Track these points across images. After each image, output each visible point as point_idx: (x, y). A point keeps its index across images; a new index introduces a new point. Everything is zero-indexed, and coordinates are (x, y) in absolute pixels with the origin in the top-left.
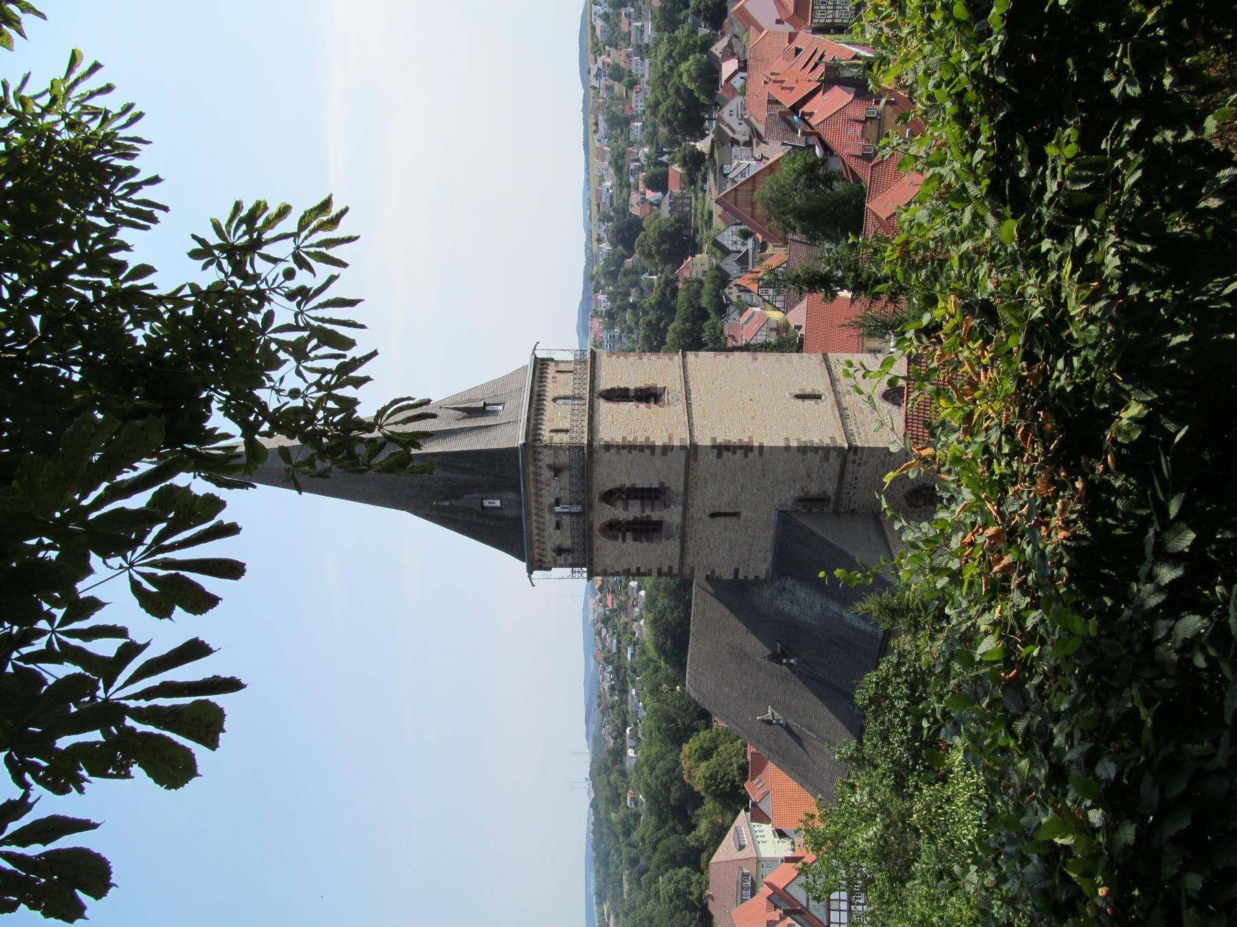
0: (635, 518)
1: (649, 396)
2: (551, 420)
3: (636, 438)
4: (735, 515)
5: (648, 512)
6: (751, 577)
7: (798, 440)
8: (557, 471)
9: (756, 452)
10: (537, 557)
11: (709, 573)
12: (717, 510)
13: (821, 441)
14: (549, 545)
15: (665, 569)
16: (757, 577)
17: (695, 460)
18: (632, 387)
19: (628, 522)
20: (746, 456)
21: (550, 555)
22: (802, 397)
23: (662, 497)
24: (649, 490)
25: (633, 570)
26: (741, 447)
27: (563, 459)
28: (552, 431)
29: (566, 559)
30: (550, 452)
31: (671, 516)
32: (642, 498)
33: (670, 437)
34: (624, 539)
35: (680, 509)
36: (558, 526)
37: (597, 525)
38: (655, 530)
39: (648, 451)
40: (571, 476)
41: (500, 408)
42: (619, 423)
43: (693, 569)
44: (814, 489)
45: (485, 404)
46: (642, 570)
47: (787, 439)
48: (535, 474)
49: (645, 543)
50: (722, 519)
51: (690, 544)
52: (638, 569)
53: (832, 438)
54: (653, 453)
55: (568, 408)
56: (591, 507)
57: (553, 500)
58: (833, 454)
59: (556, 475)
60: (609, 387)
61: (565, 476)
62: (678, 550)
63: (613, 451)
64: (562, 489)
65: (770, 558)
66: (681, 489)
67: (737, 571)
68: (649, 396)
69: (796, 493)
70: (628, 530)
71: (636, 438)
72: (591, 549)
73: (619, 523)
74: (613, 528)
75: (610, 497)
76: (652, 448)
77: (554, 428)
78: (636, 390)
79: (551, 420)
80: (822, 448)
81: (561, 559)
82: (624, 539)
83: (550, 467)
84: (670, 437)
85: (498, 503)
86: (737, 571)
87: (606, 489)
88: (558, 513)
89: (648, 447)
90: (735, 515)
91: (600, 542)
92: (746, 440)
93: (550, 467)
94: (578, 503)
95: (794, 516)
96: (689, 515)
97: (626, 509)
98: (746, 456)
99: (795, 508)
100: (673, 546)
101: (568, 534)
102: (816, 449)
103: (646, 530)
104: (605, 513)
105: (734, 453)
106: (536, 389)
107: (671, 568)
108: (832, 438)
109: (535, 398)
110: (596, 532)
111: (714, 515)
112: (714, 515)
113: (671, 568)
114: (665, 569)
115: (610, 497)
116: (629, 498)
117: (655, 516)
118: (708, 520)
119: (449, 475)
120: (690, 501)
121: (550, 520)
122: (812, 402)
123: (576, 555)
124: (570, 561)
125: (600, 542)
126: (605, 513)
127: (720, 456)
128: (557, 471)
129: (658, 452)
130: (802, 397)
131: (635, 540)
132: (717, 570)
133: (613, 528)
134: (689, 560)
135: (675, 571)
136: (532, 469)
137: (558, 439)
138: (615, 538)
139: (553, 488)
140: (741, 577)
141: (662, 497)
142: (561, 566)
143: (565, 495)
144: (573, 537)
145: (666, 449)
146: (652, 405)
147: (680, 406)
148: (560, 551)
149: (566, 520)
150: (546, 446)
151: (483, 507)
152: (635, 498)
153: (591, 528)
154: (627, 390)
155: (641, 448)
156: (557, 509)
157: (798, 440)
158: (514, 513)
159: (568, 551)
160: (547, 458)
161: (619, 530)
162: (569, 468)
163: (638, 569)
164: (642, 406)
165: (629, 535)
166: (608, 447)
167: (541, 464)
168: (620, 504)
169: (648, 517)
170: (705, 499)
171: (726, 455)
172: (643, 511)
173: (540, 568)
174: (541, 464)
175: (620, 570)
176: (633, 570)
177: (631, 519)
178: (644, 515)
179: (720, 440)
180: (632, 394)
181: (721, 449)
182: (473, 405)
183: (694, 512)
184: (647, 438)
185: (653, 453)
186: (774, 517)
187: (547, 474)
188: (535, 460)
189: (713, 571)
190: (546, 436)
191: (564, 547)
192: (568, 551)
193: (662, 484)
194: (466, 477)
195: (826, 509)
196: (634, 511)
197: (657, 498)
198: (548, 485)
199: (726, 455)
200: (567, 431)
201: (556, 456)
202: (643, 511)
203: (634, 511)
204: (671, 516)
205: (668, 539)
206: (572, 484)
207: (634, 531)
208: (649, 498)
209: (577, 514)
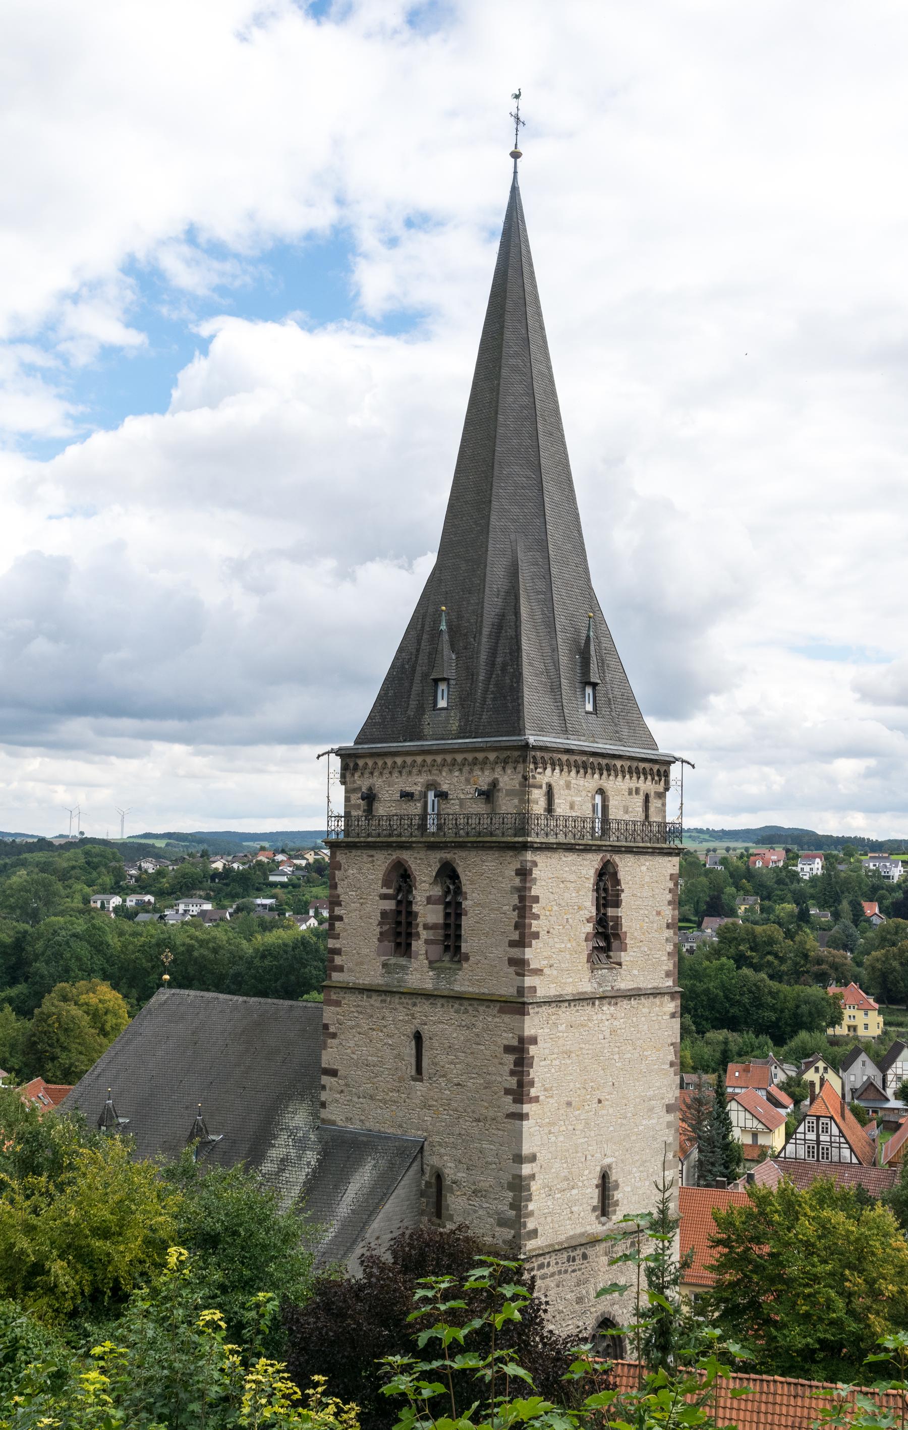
0: (416, 915)
1: (606, 937)
2: (568, 786)
3: (537, 917)
5: (424, 934)
6: (324, 1096)
7: (533, 1177)
8: (488, 795)
9: (514, 1108)
10: (361, 762)
11: (332, 1029)
12: (426, 1044)
13: (531, 1214)
14: (378, 782)
15: (338, 960)
16: (323, 1105)
17: (502, 1011)
18: (621, 912)
19: (410, 903)
20: (508, 1092)
21: (364, 783)
22: (605, 1185)
23: (447, 958)
24: (459, 937)
25: (338, 911)
26: (520, 1084)
28: (550, 787)
29: (358, 807)
31: (419, 974)
32: (446, 926)
33: (538, 972)
34: (384, 897)
35: (429, 985)
36: (407, 796)
37: (406, 856)
38: (398, 945)
39: (515, 936)
41: (589, 707)
42: (562, 888)
43: (338, 1004)
44: (456, 1203)
45: (594, 685)
46: (338, 924)
47: (533, 1158)
48: (486, 761)
49: (378, 930)
50: (409, 1050)
51: (375, 1001)
52: (340, 918)
53: (534, 1233)
54: (512, 944)
55: (588, 813)
56: (432, 846)
57: (445, 788)
58: (508, 1233)
59: (481, 793)
60: (621, 875)
61: (480, 807)
63: (517, 881)
64: (462, 802)
65: (351, 1127)
66: (457, 988)
67: (333, 1073)
68: (606, 937)
69: (451, 1172)
70: (399, 903)
71: (537, 917)
73: (410, 891)
74: (401, 879)
75: (448, 875)
76: (522, 943)
77: (555, 791)
78: (617, 920)
79: (568, 786)
80: (519, 1216)
81: (356, 799)
82: (384, 897)
83: (494, 784)
84: (538, 972)
85: (442, 703)
86: (333, 1073)
87: (460, 870)
88: (426, 796)
89: (522, 936)
91: (382, 862)
92: (533, 1092)
93: (494, 784)
94: (440, 827)
95: (415, 1167)
97: (429, 900)
98: (508, 1092)
99: (428, 1169)
100: (373, 975)
102: (518, 1205)
103: (399, 931)
105: (512, 1073)
106: (619, 763)
107: (340, 969)
108: (534, 1233)
109: (604, 762)
110: (396, 855)
111: (418, 1037)
112: (418, 1037)
113: (340, 969)
114: (338, 960)
115: (448, 875)
116: (447, 905)
117: (418, 946)
118: (410, 1029)
119: (486, 631)
120: (440, 1002)
121: (415, 783)
122: (595, 1202)
123: (363, 822)
124: (354, 813)
125: (382, 862)
126: (424, 870)
127: (508, 1049)
128: (488, 795)
129: (515, 952)
130: (605, 1185)
131: (384, 914)
132: (335, 1042)
133: (401, 879)
135: (336, 976)
136: (492, 756)
137: (538, 796)
138: (386, 883)
140: (325, 1080)
141: (447, 958)
142: (347, 799)
143: (453, 807)
144: (390, 818)
145: (520, 965)
146: (591, 944)
147: (587, 986)
148: (370, 798)
149: (415, 809)
150: (525, 778)
151: (436, 681)
152: (447, 915)
153: (402, 846)
154: (617, 904)
155: (520, 925)
156: (431, 795)
157: (533, 1177)
158: (427, 730)
159: (369, 810)
160: (508, 780)
161: (399, 890)
162: (493, 813)
163: (340, 918)
164: (589, 928)
165: (390, 905)
166: (524, 873)
167: (499, 769)
168: (437, 891)
170: (441, 1024)
171: (510, 1059)
172: (426, 927)
173: (345, 768)
174: (499, 769)
175: (340, 890)
176: (338, 911)
177: (415, 908)
178: (420, 929)
179: (533, 1050)
180: (611, 912)
181: (519, 1053)
182: (594, 667)
184: (536, 935)
185: (512, 944)
187: (483, 779)
188: (506, 762)
189: (334, 1036)
190: (546, 776)
191: (376, 805)
192: (369, 810)
193: (467, 959)
194: (483, 656)
195: (425, 1219)
196: (428, 914)
197: (447, 948)
198: (468, 781)
199: (510, 1059)
200: (550, 809)
201: (511, 793)
202: (426, 927)
203: (428, 914)
204: (419, 974)
205: (385, 965)
206: (468, 817)
207: (399, 912)
208: (447, 936)
209: (423, 827)
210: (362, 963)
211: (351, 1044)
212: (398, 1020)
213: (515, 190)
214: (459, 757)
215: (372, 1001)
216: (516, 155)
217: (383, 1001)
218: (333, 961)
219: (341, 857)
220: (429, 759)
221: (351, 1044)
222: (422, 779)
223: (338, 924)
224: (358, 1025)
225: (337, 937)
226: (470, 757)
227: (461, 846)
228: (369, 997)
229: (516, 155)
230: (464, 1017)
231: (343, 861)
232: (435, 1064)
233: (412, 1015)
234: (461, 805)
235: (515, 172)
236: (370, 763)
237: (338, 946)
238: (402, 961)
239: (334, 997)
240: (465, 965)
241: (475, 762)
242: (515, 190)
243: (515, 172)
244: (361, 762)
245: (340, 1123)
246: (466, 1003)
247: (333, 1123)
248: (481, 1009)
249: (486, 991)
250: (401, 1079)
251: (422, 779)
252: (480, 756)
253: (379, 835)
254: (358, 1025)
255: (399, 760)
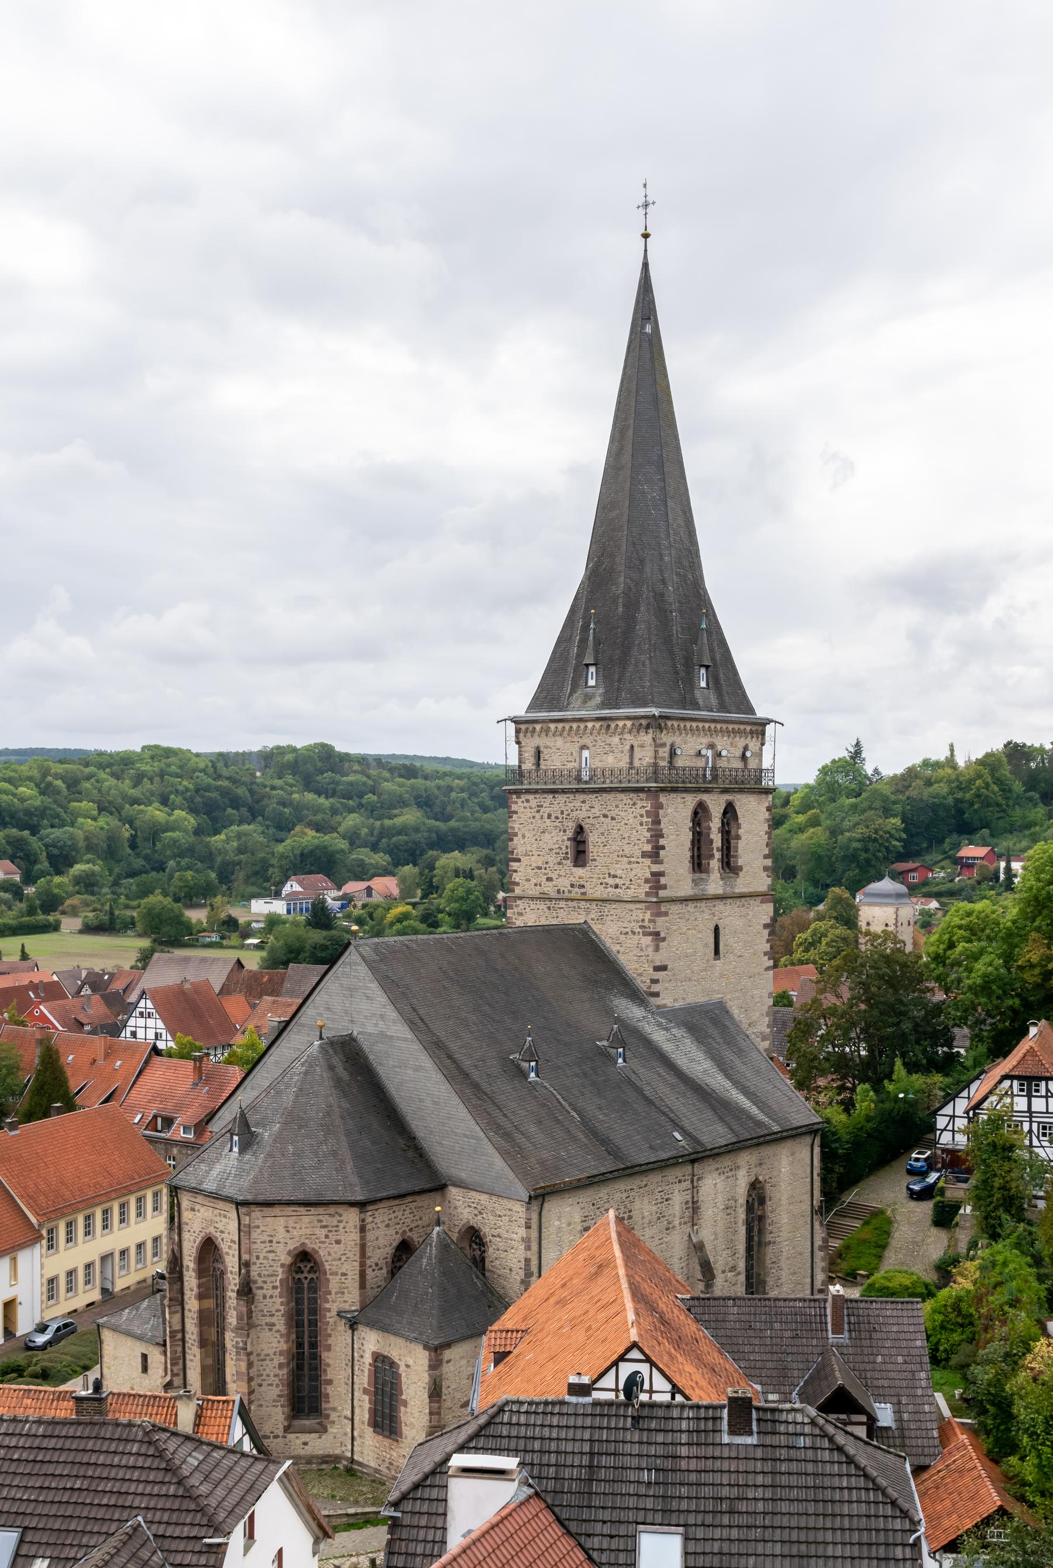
4: (717, 951)
11: (662, 935)
14: (678, 740)
25: (662, 842)
27: (752, 764)
29: (663, 759)
30: (757, 748)
31: (715, 884)
35: (720, 891)
37: (705, 797)
40: (737, 770)
43: (666, 914)
46: (662, 852)
51: (691, 907)
52: (663, 848)
57: (719, 748)
61: (739, 765)
62: (681, 893)
65: (677, 1005)
66: (739, 890)
67: (663, 968)
72: (686, 790)
75: (730, 811)
86: (663, 968)
87: (737, 808)
90: (717, 951)
91: (690, 801)
93: (746, 748)
94: (715, 777)
96: (717, 902)
100: (686, 889)
101: (688, 764)
104: (716, 805)
107: (665, 887)
111: (717, 929)
112: (717, 929)
113: (665, 887)
115: (730, 811)
120: (729, 901)
125: (690, 801)
127: (766, 926)
134: (674, 908)
135: (662, 893)
136: (748, 728)
139: (729, 749)
143: (722, 763)
144: (691, 769)
153: (707, 791)
163: (663, 848)
169: (712, 856)
170: (730, 916)
171: (767, 932)
175: (662, 826)
176: (662, 842)
183: (720, 906)
185: (766, 857)
186: (716, 997)
189: (664, 939)
193: (741, 868)
198: (732, 744)
204: (715, 884)
210: (679, 881)
211: (676, 943)
212: (703, 918)
213: (646, 265)
214: (731, 727)
215: (689, 908)
216: (646, 236)
217: (696, 907)
218: (659, 881)
219: (663, 798)
220: (713, 726)
221: (676, 943)
222: (705, 740)
223: (662, 852)
224: (680, 928)
225: (661, 862)
226: (736, 727)
227: (741, 791)
228: (687, 905)
229: (646, 236)
230: (742, 909)
231: (664, 802)
232: (726, 945)
233: (714, 914)
234: (728, 761)
235: (646, 251)
236: (676, 724)
237: (662, 869)
238: (703, 875)
239: (663, 909)
240: (741, 874)
241: (739, 732)
242: (646, 265)
243: (646, 251)
244: (669, 723)
245: (669, 1005)
246: (743, 900)
247: (665, 1006)
248: (752, 902)
249: (752, 890)
250: (708, 961)
251: (705, 740)
252: (742, 727)
253: (638, 782)
254: (680, 928)
255: (694, 725)
